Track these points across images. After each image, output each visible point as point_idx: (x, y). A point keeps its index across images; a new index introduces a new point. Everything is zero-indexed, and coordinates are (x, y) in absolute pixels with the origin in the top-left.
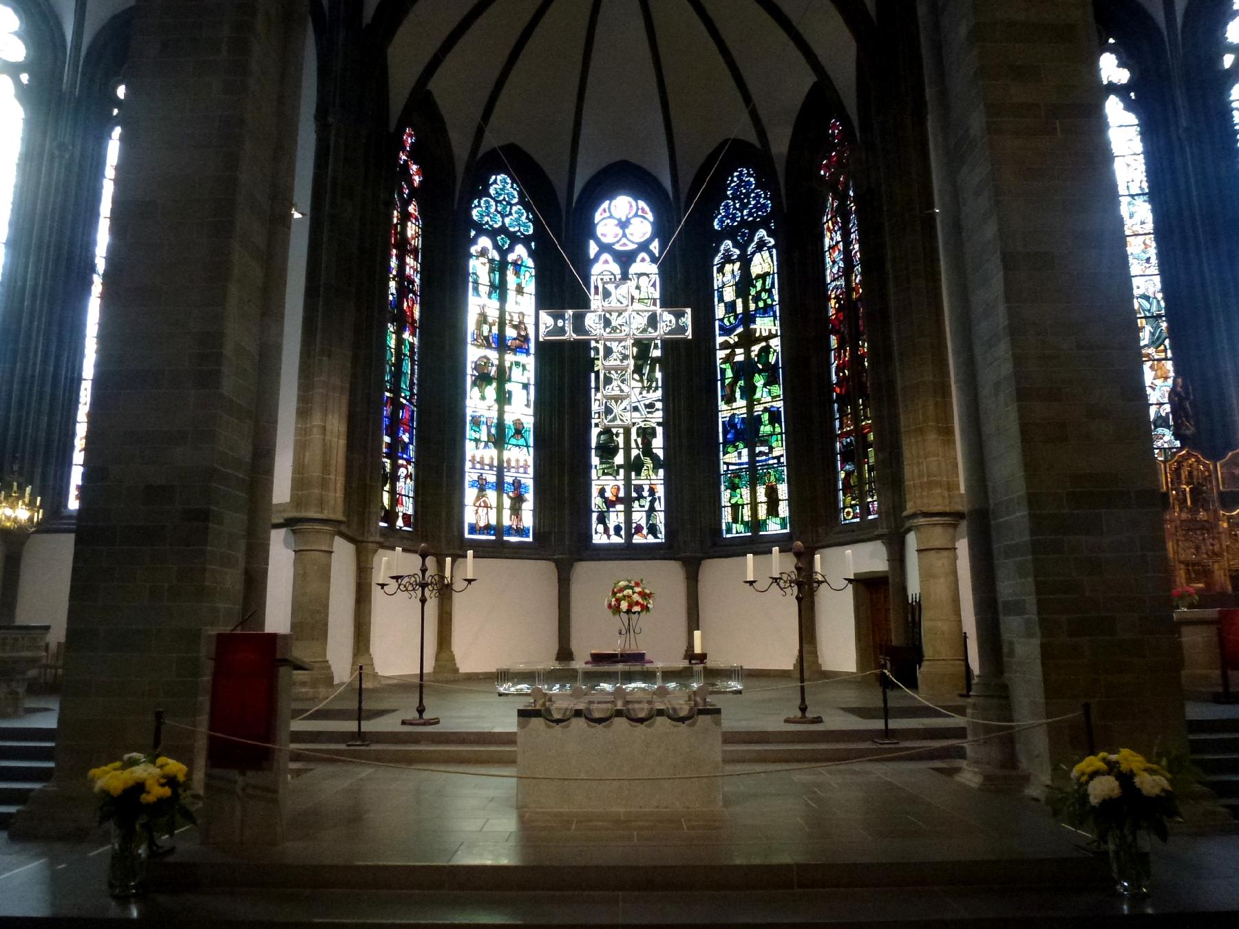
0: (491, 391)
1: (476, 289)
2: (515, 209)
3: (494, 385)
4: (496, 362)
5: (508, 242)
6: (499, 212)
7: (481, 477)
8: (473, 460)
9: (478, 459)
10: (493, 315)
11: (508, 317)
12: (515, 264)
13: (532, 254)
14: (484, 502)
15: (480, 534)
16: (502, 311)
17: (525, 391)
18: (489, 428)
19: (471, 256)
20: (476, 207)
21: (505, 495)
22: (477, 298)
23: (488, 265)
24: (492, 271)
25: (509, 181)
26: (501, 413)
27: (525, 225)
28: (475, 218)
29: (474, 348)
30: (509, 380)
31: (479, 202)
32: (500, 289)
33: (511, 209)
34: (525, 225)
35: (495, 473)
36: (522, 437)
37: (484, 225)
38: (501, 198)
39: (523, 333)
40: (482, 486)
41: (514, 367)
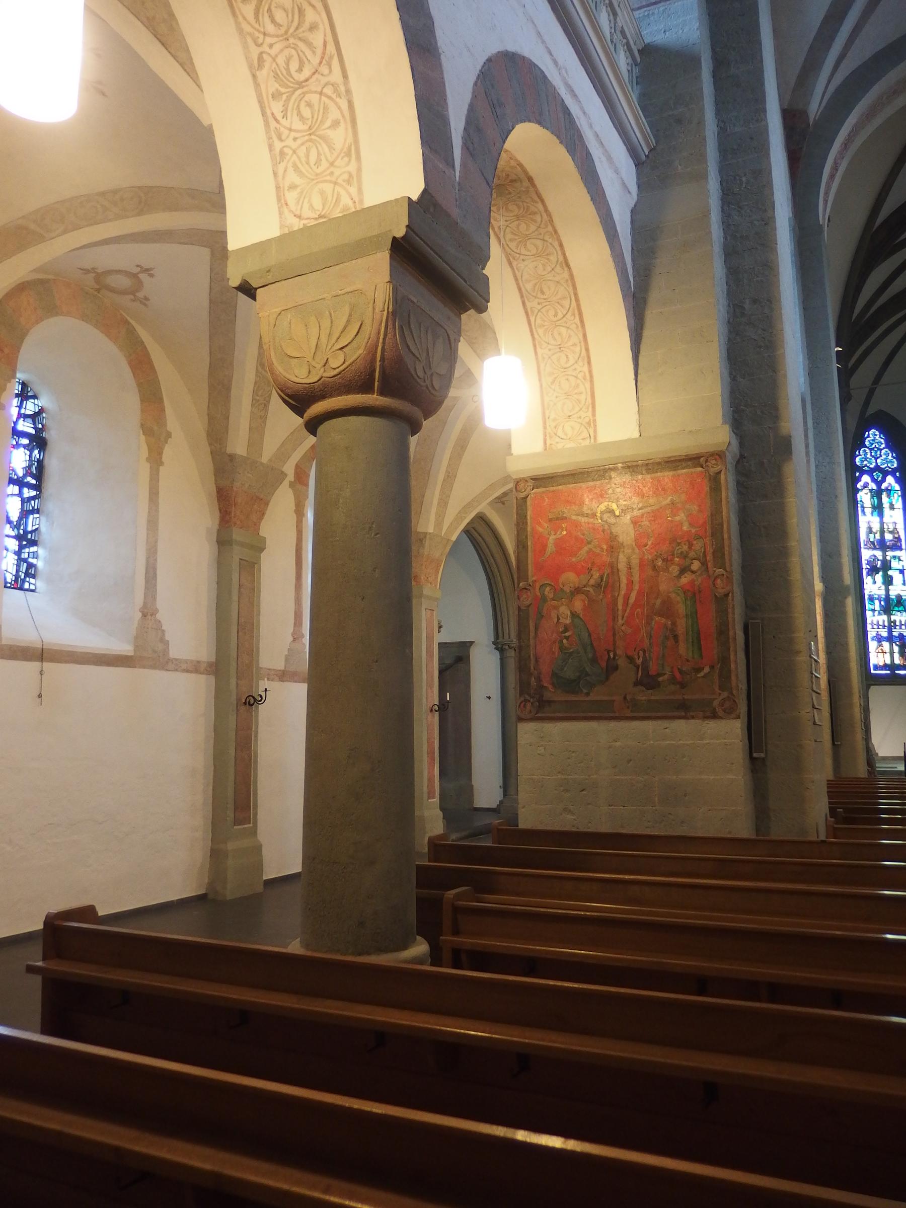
0: (879, 577)
1: (863, 511)
2: (883, 451)
3: (881, 573)
4: (881, 558)
5: (881, 476)
6: (873, 456)
7: (877, 634)
8: (872, 624)
9: (875, 622)
10: (876, 527)
11: (885, 526)
12: (887, 489)
13: (897, 480)
14: (882, 649)
15: (880, 670)
16: (882, 523)
17: (901, 575)
18: (880, 601)
19: (858, 490)
20: (858, 456)
21: (894, 644)
22: (864, 517)
23: (869, 494)
24: (872, 497)
25: (877, 433)
26: (887, 591)
27: (891, 462)
28: (858, 464)
29: (866, 550)
30: (890, 568)
31: (859, 452)
32: (878, 508)
33: (881, 452)
34: (891, 462)
35: (886, 630)
36: (902, 605)
37: (864, 467)
38: (873, 446)
39: (896, 536)
40: (879, 639)
41: (892, 560)
